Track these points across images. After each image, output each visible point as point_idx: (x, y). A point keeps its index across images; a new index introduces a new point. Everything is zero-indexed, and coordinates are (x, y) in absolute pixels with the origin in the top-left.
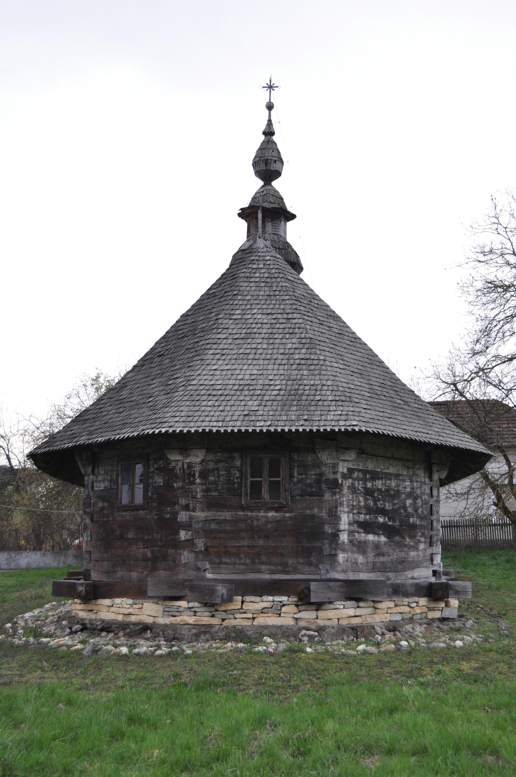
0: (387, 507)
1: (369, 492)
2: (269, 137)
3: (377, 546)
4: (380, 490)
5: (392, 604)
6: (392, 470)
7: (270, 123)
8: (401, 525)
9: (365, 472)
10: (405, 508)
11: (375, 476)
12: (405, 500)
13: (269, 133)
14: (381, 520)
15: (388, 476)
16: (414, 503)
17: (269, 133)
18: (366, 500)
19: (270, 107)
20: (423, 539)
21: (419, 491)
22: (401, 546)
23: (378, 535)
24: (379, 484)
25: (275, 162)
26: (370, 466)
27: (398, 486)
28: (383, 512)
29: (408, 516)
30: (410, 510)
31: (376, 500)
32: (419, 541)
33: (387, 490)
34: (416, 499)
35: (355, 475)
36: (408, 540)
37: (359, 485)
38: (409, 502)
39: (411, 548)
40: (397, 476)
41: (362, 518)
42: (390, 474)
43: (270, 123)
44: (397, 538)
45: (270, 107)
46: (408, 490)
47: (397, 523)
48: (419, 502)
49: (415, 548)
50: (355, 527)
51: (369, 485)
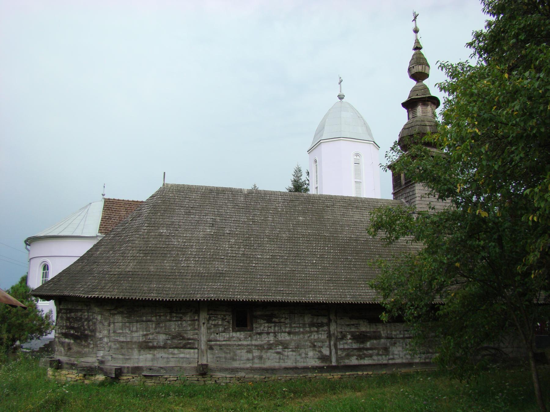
0: (75, 326)
1: (68, 319)
2: (417, 51)
3: (69, 344)
4: (72, 318)
5: (67, 373)
6: (79, 307)
7: (417, 42)
8: (81, 335)
9: (67, 309)
10: (83, 326)
11: (71, 311)
12: (84, 322)
13: (417, 48)
14: (72, 332)
15: (77, 311)
16: (88, 324)
17: (417, 48)
18: (66, 323)
19: (416, 31)
20: (91, 342)
21: (91, 317)
22: (80, 345)
23: (70, 339)
24: (73, 314)
25: (413, 67)
26: (70, 307)
27: (81, 315)
28: (73, 328)
29: (85, 330)
30: (86, 327)
31: (70, 323)
32: (90, 343)
33: (76, 318)
34: (89, 321)
35: (63, 311)
36: (84, 342)
37: (64, 316)
38: (86, 323)
39: (84, 346)
40: (81, 310)
41: (64, 331)
42: (78, 310)
43: (417, 42)
44: (79, 341)
45: (416, 31)
46: (86, 317)
47: (79, 334)
48: (91, 323)
49: (88, 346)
50: (61, 335)
51: (68, 315)
